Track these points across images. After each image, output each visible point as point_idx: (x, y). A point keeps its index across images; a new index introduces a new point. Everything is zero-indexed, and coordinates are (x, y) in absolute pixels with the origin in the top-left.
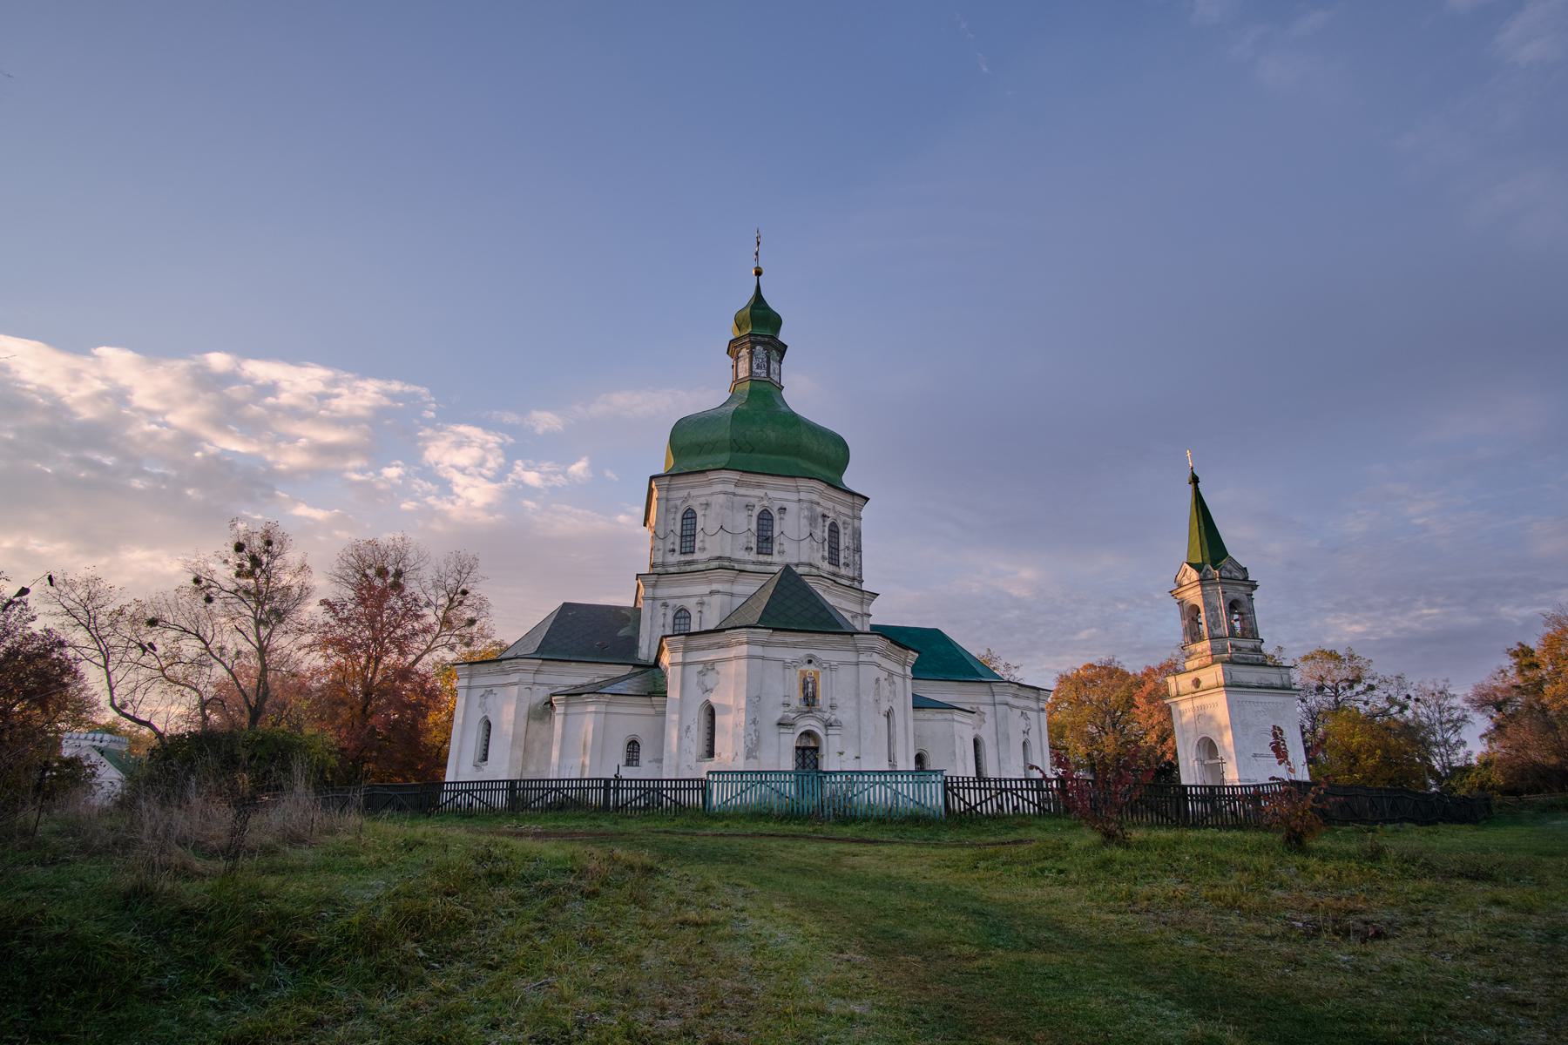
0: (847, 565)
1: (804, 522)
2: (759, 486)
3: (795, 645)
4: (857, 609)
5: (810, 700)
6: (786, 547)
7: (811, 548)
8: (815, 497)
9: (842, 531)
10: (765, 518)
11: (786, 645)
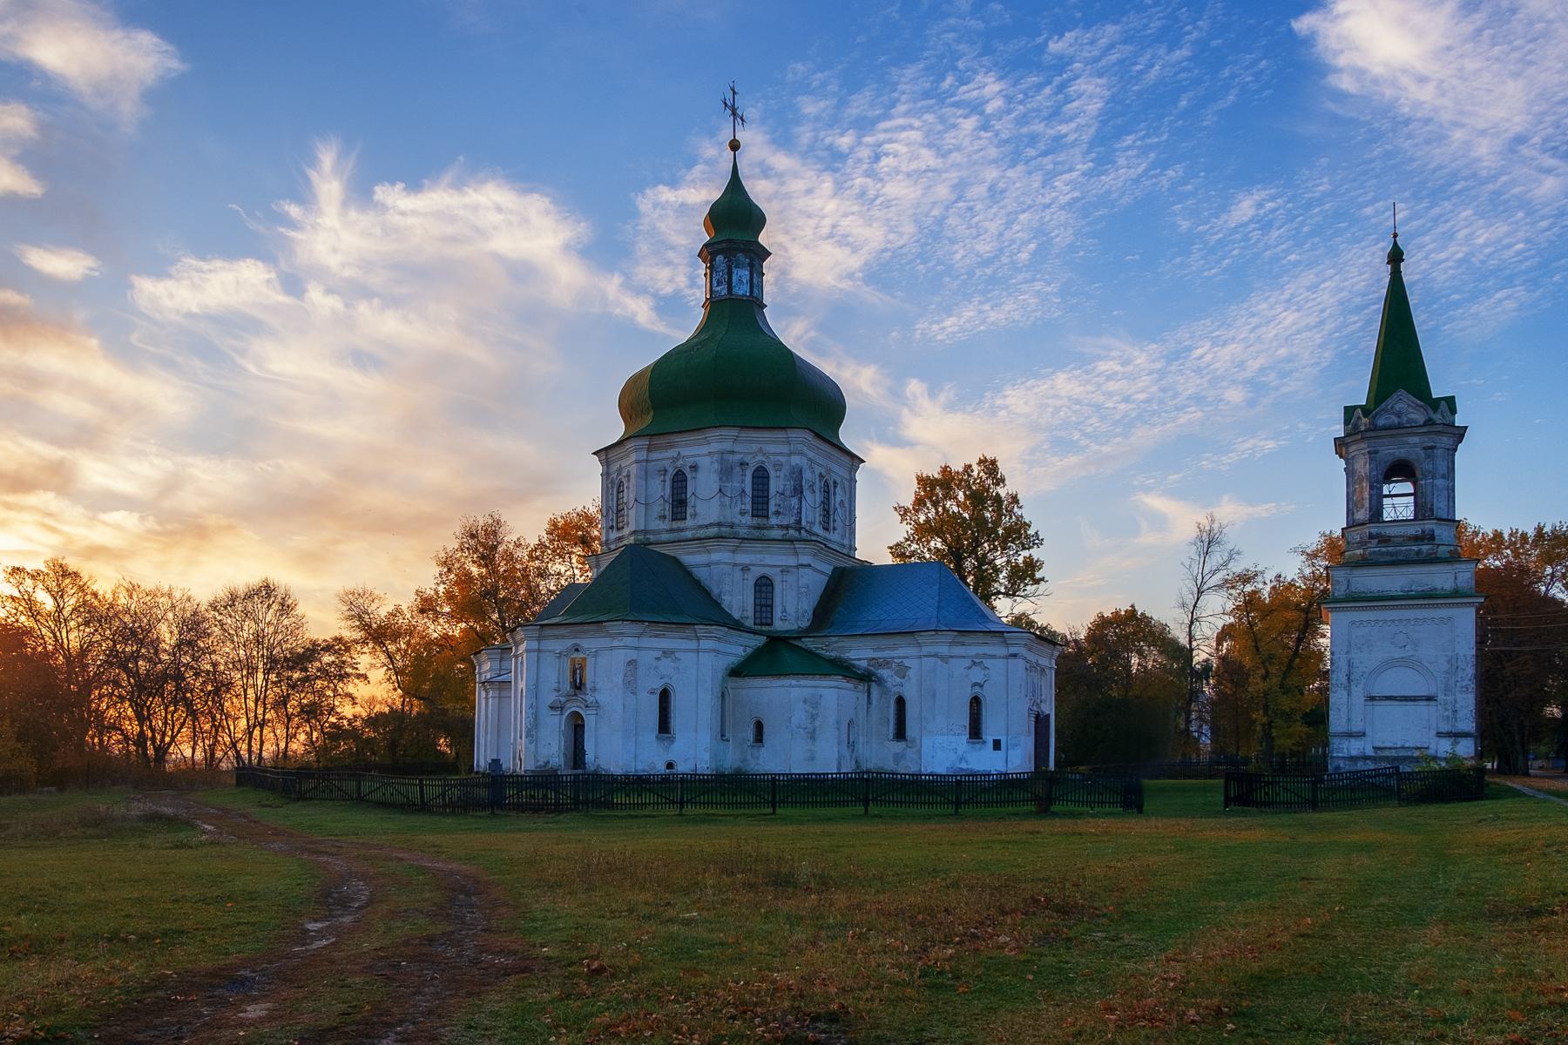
0: (777, 513)
1: (715, 477)
3: (563, 637)
4: (791, 561)
5: (578, 686)
6: (698, 510)
7: (722, 505)
8: (727, 446)
9: (772, 474)
10: (679, 481)
11: (556, 637)
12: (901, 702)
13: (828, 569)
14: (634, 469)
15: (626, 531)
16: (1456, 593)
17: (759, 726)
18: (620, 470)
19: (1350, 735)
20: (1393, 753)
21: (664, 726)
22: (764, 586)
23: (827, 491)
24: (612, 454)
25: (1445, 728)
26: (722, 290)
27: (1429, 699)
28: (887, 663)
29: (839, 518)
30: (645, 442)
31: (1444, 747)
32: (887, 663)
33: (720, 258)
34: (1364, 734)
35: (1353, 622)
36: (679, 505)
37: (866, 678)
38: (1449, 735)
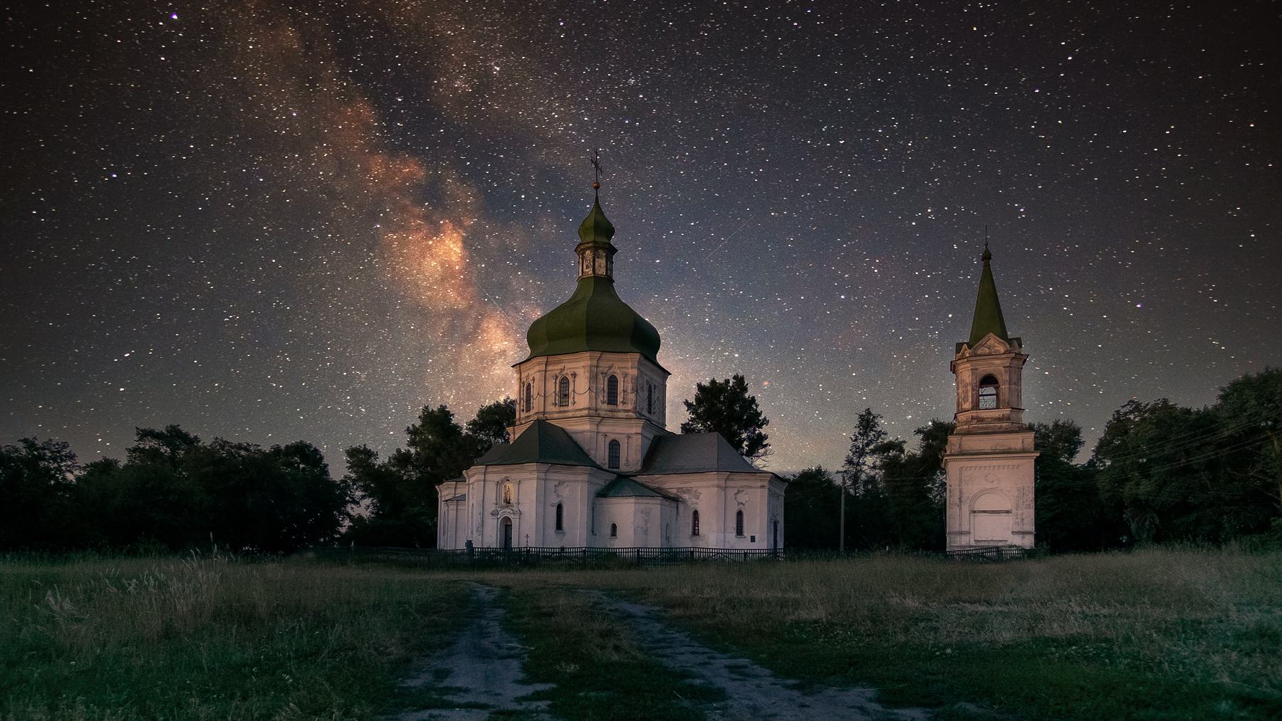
0: (623, 403)
2: (560, 362)
3: (499, 472)
10: (564, 383)
12: (696, 513)
13: (651, 437)
14: (537, 376)
15: (532, 412)
16: (1024, 451)
17: (614, 527)
18: (528, 377)
19: (961, 533)
20: (986, 544)
21: (559, 526)
22: (614, 446)
23: (650, 391)
24: (523, 367)
25: (1017, 529)
26: (590, 271)
27: (1008, 512)
28: (688, 491)
29: (656, 406)
30: (544, 359)
31: (1017, 541)
32: (688, 491)
33: (588, 252)
34: (969, 533)
35: (961, 469)
36: (564, 396)
37: (675, 500)
38: (1018, 533)
